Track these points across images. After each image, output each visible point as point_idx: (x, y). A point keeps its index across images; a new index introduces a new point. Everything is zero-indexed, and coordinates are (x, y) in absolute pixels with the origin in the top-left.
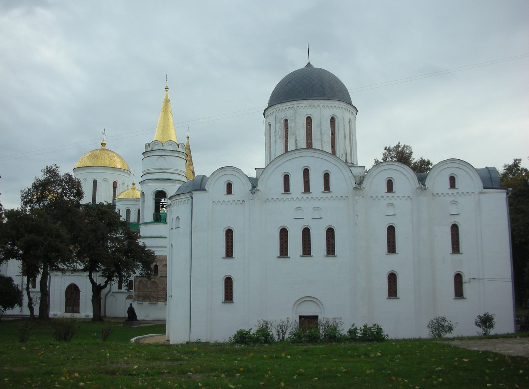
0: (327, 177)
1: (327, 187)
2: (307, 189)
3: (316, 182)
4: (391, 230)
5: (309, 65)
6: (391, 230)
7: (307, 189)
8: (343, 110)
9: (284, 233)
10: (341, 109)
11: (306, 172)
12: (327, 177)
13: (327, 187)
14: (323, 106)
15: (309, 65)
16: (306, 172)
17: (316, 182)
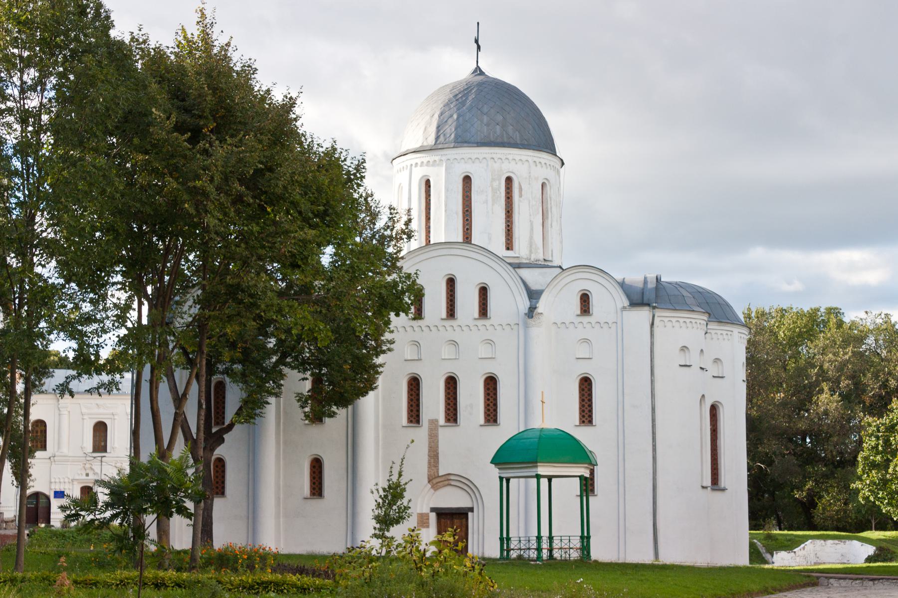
0: (484, 292)
1: (484, 311)
2: (451, 313)
3: (467, 301)
4: (586, 384)
5: (478, 71)
6: (586, 384)
7: (451, 313)
8: (530, 167)
10: (526, 164)
11: (451, 283)
12: (484, 292)
13: (484, 311)
15: (478, 71)
16: (451, 283)
17: (467, 301)
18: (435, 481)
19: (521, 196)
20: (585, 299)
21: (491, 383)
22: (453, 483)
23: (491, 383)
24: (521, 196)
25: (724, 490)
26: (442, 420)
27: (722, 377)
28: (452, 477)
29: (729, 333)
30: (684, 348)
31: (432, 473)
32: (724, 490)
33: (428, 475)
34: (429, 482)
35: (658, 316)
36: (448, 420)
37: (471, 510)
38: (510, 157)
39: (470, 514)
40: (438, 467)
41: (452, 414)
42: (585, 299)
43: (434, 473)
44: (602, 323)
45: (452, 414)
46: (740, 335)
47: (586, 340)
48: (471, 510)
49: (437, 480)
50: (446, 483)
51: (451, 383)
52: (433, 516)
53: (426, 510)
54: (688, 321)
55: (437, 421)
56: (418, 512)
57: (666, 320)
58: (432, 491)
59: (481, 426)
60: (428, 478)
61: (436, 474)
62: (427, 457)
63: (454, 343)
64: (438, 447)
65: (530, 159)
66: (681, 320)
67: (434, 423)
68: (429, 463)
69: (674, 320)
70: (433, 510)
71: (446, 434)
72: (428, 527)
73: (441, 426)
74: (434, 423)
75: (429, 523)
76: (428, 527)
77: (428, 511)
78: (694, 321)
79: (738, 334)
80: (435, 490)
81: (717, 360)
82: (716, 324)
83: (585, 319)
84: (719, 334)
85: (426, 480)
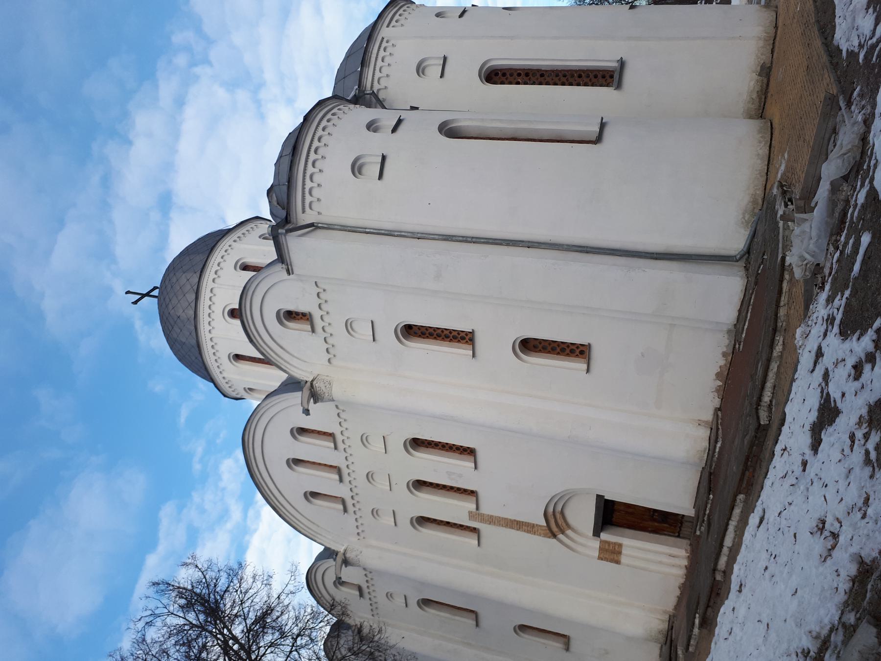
4: (410, 331)
9: (423, 521)
14: (210, 331)
22: (559, 508)
25: (622, 63)
27: (445, 59)
28: (551, 510)
29: (384, 44)
30: (357, 168)
31: (542, 532)
32: (622, 63)
33: (544, 537)
34: (554, 536)
35: (304, 212)
37: (599, 498)
39: (606, 498)
40: (534, 524)
43: (541, 530)
44: (320, 301)
46: (393, 23)
47: (349, 326)
48: (599, 498)
50: (558, 516)
52: (604, 536)
53: (596, 544)
54: (313, 156)
55: (470, 513)
56: (597, 554)
57: (308, 199)
59: (476, 468)
60: (549, 537)
61: (544, 528)
62: (519, 532)
63: (369, 477)
66: (310, 169)
68: (528, 532)
69: (309, 184)
70: (596, 533)
72: (620, 545)
73: (477, 508)
76: (620, 545)
78: (316, 144)
79: (390, 27)
80: (569, 526)
81: (421, 69)
82: (366, 70)
84: (382, 64)
85: (554, 540)
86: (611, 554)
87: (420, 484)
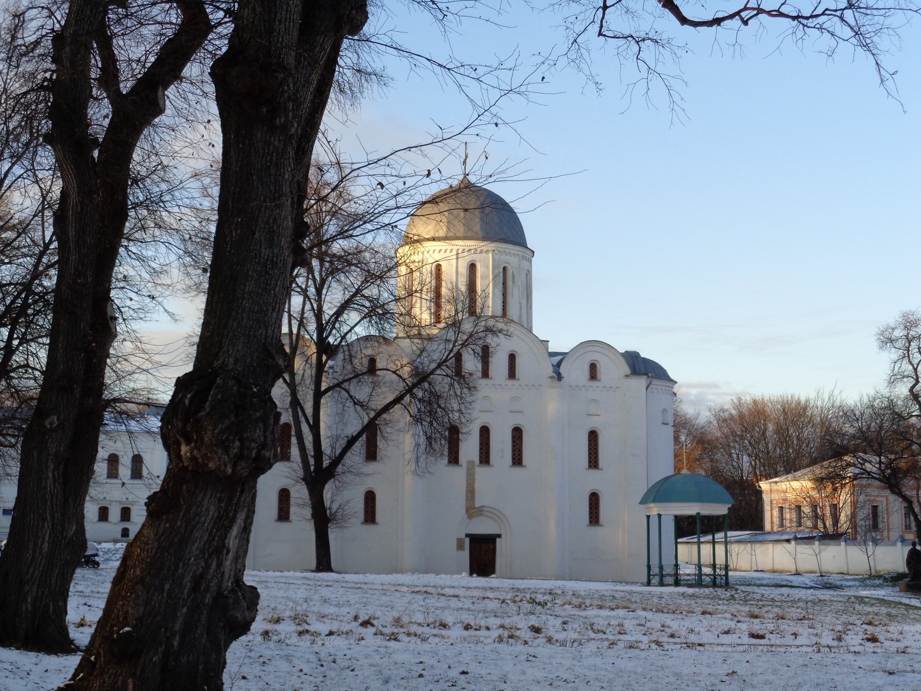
0: (512, 358)
1: (512, 374)
4: (593, 437)
6: (593, 437)
13: (512, 374)
18: (471, 512)
19: (513, 283)
20: (593, 367)
21: (517, 433)
22: (485, 513)
23: (517, 433)
24: (513, 283)
26: (477, 462)
28: (485, 509)
34: (467, 511)
36: (481, 462)
37: (499, 536)
38: (507, 251)
39: (498, 539)
41: (485, 457)
42: (593, 367)
45: (485, 457)
47: (594, 401)
48: (499, 536)
49: (472, 511)
51: (485, 432)
52: (467, 540)
58: (468, 520)
64: (474, 483)
65: (520, 253)
67: (471, 464)
68: (467, 497)
70: (467, 535)
71: (481, 472)
72: (463, 549)
74: (471, 464)
75: (464, 546)
76: (463, 549)
77: (464, 536)
83: (594, 384)
85: (464, 511)
86: (460, 546)
87: (485, 432)
